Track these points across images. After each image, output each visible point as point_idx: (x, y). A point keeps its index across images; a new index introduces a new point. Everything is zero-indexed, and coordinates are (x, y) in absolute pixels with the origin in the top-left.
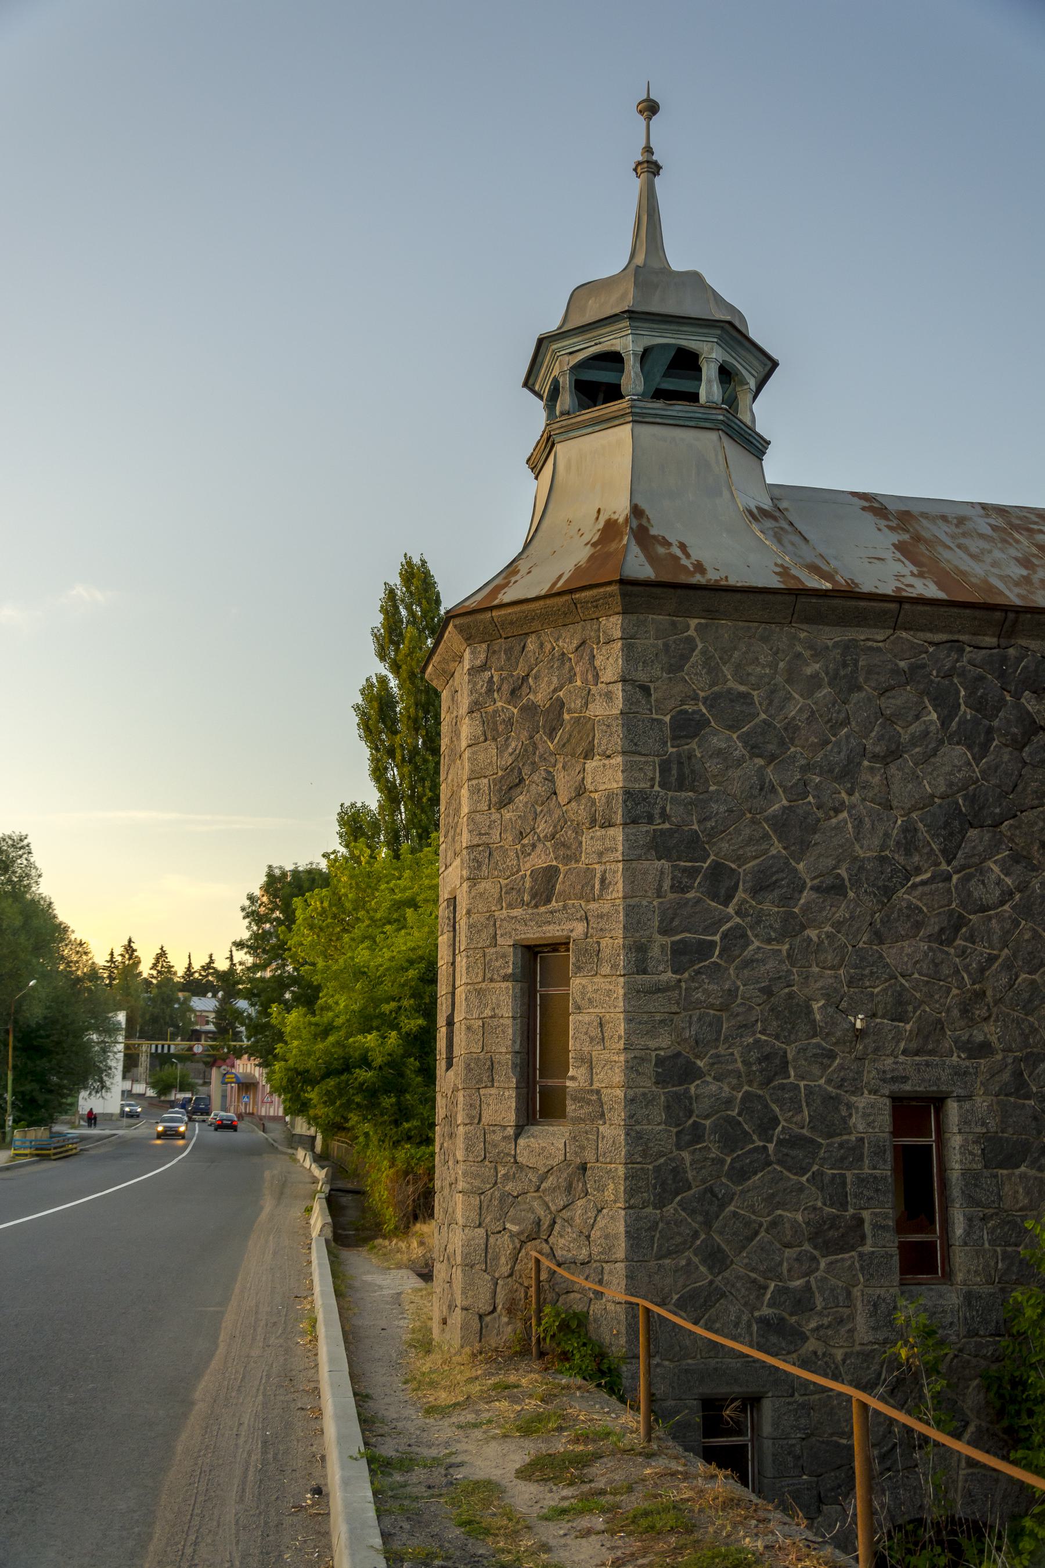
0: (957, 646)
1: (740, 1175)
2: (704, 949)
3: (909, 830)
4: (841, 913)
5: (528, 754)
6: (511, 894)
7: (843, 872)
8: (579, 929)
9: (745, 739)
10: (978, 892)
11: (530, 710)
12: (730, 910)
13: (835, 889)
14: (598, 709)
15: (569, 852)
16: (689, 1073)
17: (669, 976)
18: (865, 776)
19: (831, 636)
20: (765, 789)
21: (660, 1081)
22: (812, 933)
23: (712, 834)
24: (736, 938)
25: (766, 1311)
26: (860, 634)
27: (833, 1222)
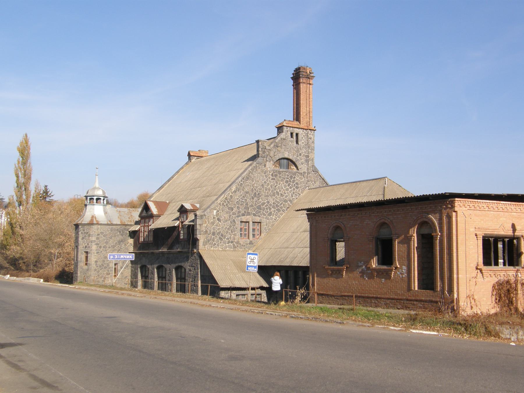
0: (121, 227)
1: (101, 269)
2: (99, 252)
3: (116, 243)
4: (110, 249)
5: (85, 236)
6: (83, 247)
7: (110, 246)
8: (89, 251)
9: (103, 236)
10: (121, 248)
11: (85, 232)
12: (101, 249)
13: (110, 247)
14: (91, 233)
15: (88, 244)
16: (97, 262)
17: (96, 254)
18: (113, 238)
19: (111, 227)
20: (104, 240)
21: (95, 262)
22: (108, 251)
23: (100, 243)
24: (101, 252)
25: (102, 279)
26: (113, 227)
27: (108, 273)
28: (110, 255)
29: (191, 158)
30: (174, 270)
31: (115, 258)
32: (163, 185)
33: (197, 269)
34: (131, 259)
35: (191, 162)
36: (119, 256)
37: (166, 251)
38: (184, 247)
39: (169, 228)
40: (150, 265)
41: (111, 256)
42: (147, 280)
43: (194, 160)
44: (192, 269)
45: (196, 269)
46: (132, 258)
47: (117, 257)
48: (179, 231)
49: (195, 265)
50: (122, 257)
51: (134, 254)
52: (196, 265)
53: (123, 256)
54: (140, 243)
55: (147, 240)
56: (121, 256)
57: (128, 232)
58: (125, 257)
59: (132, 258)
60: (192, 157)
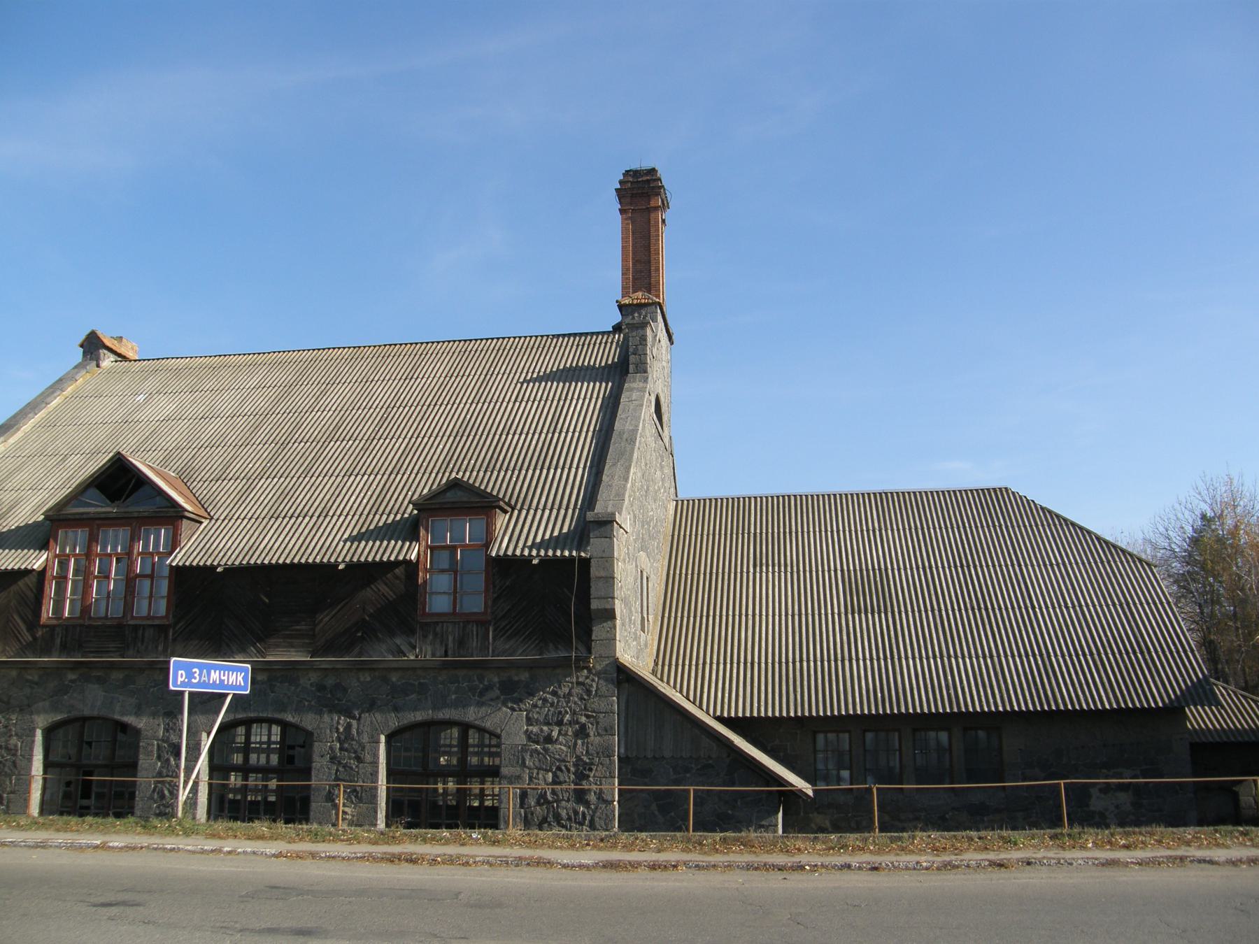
28: (179, 666)
29: (102, 355)
30: (383, 738)
31: (193, 681)
32: (15, 416)
33: (599, 735)
34: (239, 687)
35: (98, 366)
36: (205, 671)
37: (309, 659)
38: (461, 643)
39: (351, 566)
40: (154, 715)
41: (180, 672)
42: (81, 778)
43: (108, 361)
44: (555, 734)
45: (592, 730)
46: (242, 684)
47: (200, 675)
48: (420, 581)
49: (583, 719)
50: (215, 676)
51: (249, 666)
52: (587, 717)
53: (218, 672)
54: (45, 626)
55: (116, 610)
56: (213, 671)
58: (223, 678)
59: (242, 684)
60: (106, 352)
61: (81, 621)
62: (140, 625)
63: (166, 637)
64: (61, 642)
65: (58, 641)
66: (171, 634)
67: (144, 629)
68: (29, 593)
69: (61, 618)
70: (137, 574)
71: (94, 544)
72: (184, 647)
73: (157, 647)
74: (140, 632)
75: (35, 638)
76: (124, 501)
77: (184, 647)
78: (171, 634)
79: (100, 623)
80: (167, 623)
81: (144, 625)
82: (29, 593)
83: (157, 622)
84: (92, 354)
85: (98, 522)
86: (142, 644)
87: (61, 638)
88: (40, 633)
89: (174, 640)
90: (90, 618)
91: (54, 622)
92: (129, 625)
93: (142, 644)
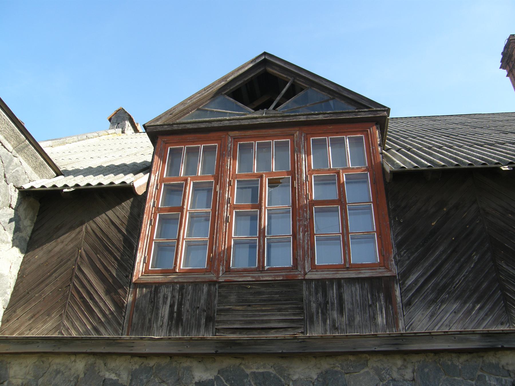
54: (139, 285)
57: (15, 195)
61: (212, 277)
62: (331, 280)
63: (390, 298)
64: (171, 312)
65: (165, 311)
66: (398, 293)
67: (340, 286)
68: (113, 233)
69: (174, 272)
70: (312, 200)
71: (229, 161)
72: (432, 316)
73: (373, 318)
74: (333, 293)
75: (120, 306)
76: (274, 109)
77: (432, 316)
78: (398, 293)
79: (249, 279)
80: (388, 274)
81: (339, 280)
82: (113, 233)
83: (366, 274)
84: (118, 124)
85: (236, 133)
86: (341, 311)
87: (172, 306)
88: (130, 298)
89: (409, 304)
90: (228, 270)
91: (159, 278)
92: (312, 280)
93: (341, 311)
